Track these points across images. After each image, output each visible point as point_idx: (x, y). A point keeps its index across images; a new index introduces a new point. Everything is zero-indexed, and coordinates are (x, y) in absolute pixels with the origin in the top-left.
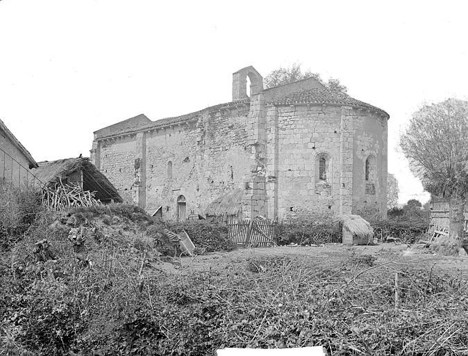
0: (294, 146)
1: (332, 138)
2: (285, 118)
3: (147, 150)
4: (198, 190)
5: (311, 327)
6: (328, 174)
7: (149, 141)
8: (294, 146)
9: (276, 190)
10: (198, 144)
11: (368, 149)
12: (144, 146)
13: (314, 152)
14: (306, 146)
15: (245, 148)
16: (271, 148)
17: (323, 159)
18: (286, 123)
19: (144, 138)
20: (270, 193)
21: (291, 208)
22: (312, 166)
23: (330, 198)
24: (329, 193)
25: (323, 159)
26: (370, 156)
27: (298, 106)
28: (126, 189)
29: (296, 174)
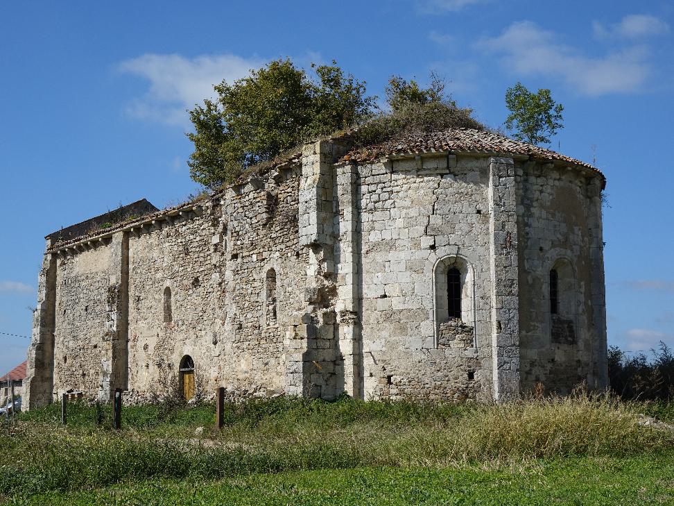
0: (391, 245)
1: (471, 225)
2: (372, 188)
3: (131, 266)
4: (215, 343)
5: (472, 437)
6: (466, 304)
7: (136, 245)
8: (391, 245)
9: (357, 339)
10: (215, 250)
11: (553, 245)
12: (125, 260)
13: (433, 258)
14: (417, 245)
15: (298, 255)
16: (346, 249)
17: (452, 276)
18: (375, 197)
19: (125, 246)
20: (346, 347)
21: (389, 377)
22: (426, 290)
23: (470, 353)
24: (469, 342)
25: (452, 276)
26: (560, 262)
27: (398, 161)
28: (95, 347)
29: (397, 304)
